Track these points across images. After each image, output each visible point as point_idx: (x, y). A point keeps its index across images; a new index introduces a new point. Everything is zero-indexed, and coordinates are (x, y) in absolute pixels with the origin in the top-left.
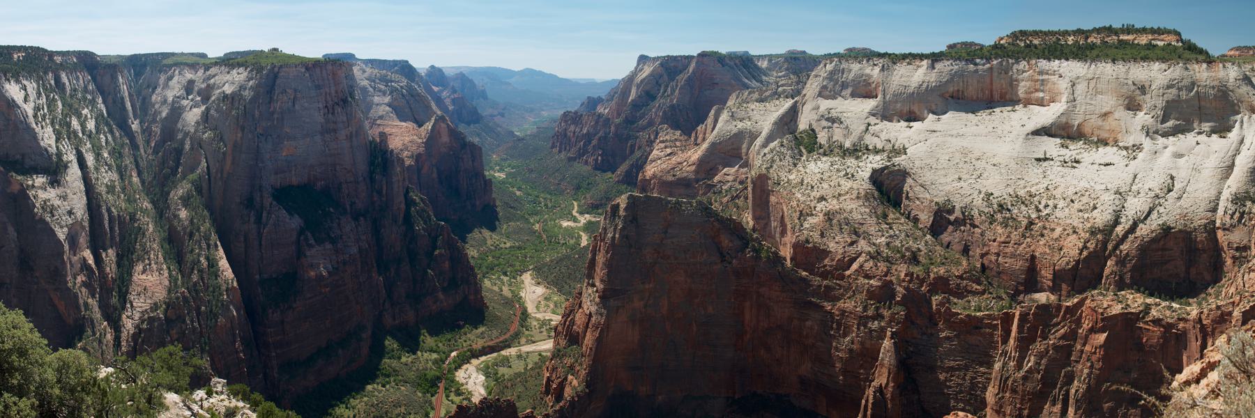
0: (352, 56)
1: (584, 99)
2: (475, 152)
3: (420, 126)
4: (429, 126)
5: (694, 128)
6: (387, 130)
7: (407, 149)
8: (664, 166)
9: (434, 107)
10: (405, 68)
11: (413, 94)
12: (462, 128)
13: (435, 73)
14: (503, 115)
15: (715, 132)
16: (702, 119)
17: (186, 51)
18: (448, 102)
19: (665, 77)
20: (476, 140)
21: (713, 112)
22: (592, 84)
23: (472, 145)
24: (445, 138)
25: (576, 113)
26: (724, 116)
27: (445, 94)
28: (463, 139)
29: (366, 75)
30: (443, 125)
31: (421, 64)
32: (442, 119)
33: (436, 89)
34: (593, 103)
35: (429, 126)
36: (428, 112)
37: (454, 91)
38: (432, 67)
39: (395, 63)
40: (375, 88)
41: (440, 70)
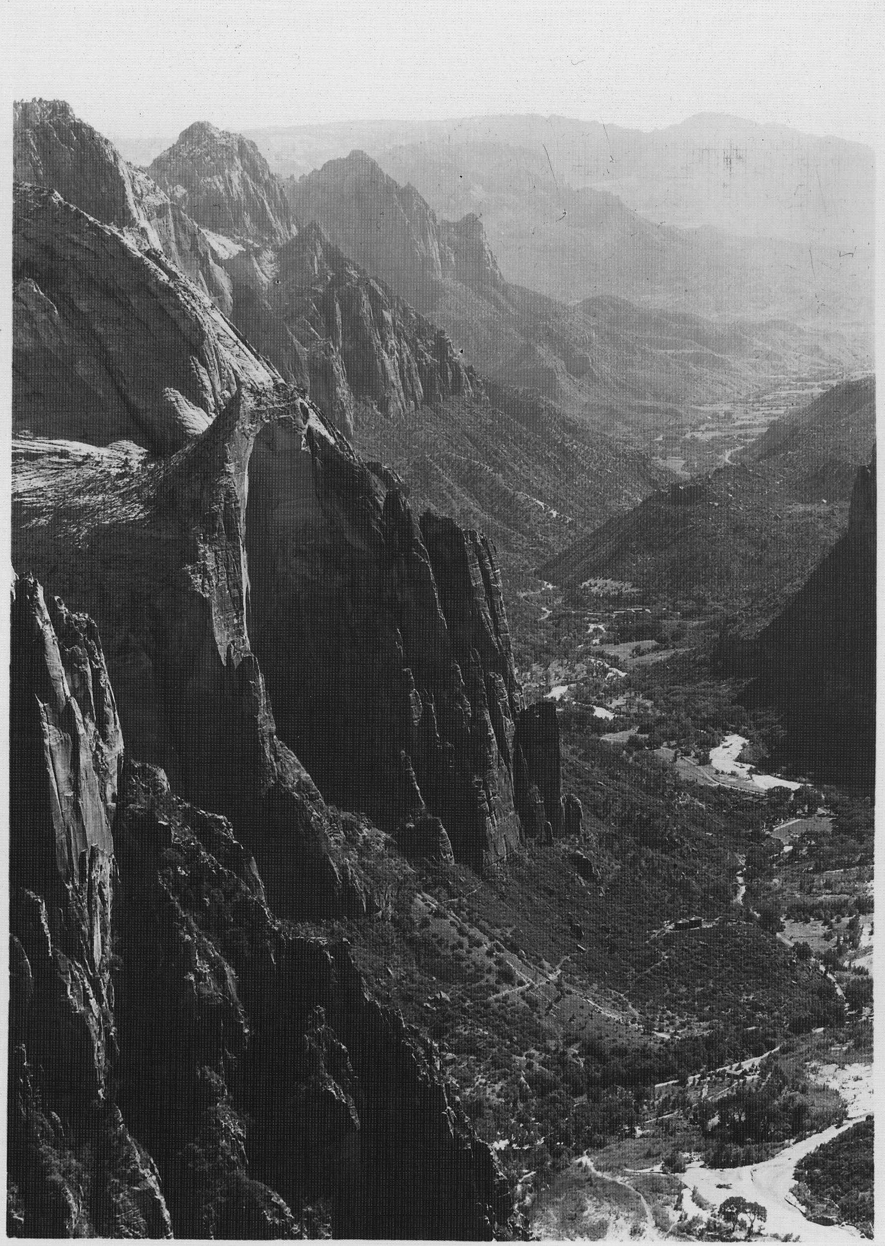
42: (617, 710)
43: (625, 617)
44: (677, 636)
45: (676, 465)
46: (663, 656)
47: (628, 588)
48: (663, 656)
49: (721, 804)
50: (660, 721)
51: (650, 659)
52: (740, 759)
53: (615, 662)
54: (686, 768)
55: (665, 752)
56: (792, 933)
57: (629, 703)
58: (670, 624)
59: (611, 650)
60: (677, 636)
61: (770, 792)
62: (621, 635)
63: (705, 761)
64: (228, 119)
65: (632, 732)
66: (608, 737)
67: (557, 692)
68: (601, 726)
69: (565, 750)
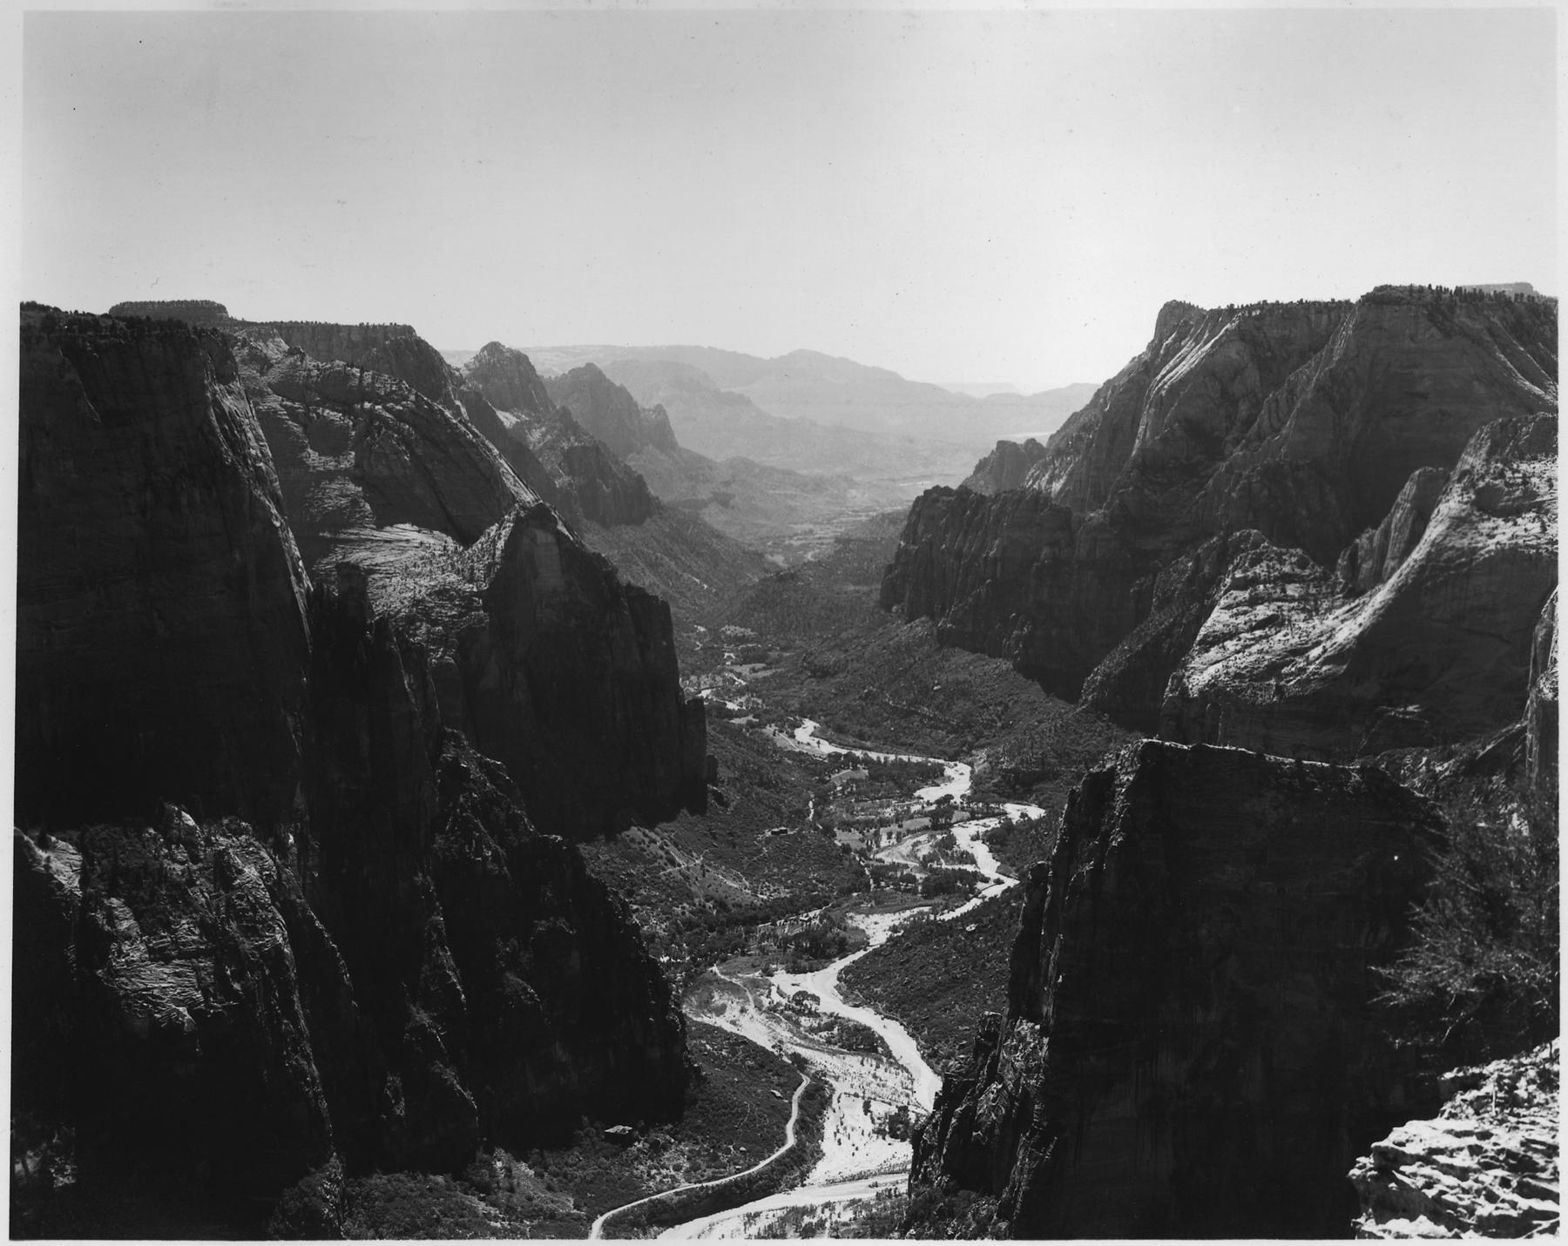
0: (212, 311)
1: (987, 447)
2: (650, 617)
3: (466, 539)
4: (498, 535)
5: (1346, 540)
6: (359, 556)
7: (426, 614)
8: (1245, 660)
9: (510, 480)
10: (402, 351)
11: (431, 433)
12: (594, 541)
13: (505, 369)
14: (724, 501)
15: (1418, 554)
16: (1375, 513)
17: (248, 319)
18: (550, 463)
19: (1253, 376)
20: (647, 581)
21: (1409, 489)
22: (1009, 402)
23: (639, 597)
24: (551, 576)
25: (964, 490)
26: (1452, 504)
27: (535, 436)
28: (611, 575)
29: (273, 376)
30: (542, 537)
31: (456, 341)
32: (538, 517)
33: (507, 419)
34: (1010, 458)
35: (498, 535)
36: (494, 500)
37: (568, 425)
38: (494, 348)
39: (368, 336)
40: (305, 422)
41: (520, 359)
42: (741, 704)
43: (749, 649)
44: (778, 661)
45: (779, 559)
46: (768, 673)
47: (749, 632)
48: (768, 673)
49: (802, 761)
50: (766, 712)
51: (760, 675)
52: (812, 735)
53: (739, 675)
54: (782, 740)
55: (769, 730)
56: (842, 838)
57: (748, 701)
58: (774, 654)
59: (738, 669)
60: (778, 661)
61: (829, 755)
62: (745, 661)
63: (792, 736)
64: (511, 342)
65: (750, 717)
66: (736, 721)
67: (704, 694)
68: (732, 714)
69: (708, 728)
